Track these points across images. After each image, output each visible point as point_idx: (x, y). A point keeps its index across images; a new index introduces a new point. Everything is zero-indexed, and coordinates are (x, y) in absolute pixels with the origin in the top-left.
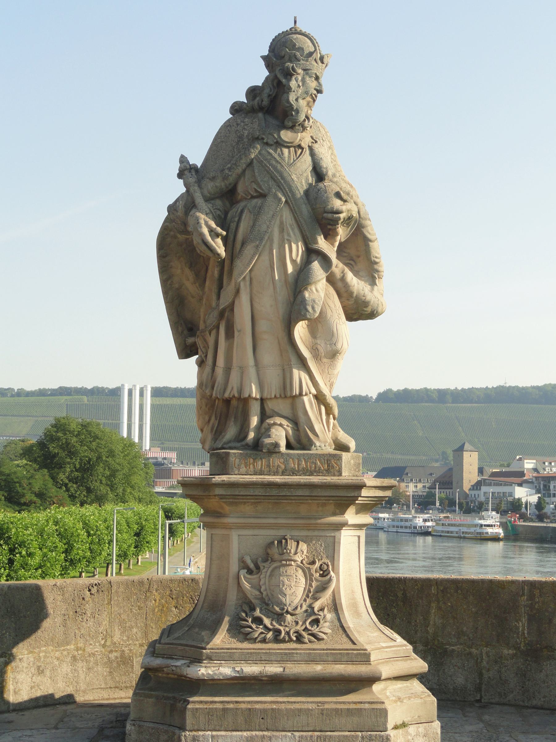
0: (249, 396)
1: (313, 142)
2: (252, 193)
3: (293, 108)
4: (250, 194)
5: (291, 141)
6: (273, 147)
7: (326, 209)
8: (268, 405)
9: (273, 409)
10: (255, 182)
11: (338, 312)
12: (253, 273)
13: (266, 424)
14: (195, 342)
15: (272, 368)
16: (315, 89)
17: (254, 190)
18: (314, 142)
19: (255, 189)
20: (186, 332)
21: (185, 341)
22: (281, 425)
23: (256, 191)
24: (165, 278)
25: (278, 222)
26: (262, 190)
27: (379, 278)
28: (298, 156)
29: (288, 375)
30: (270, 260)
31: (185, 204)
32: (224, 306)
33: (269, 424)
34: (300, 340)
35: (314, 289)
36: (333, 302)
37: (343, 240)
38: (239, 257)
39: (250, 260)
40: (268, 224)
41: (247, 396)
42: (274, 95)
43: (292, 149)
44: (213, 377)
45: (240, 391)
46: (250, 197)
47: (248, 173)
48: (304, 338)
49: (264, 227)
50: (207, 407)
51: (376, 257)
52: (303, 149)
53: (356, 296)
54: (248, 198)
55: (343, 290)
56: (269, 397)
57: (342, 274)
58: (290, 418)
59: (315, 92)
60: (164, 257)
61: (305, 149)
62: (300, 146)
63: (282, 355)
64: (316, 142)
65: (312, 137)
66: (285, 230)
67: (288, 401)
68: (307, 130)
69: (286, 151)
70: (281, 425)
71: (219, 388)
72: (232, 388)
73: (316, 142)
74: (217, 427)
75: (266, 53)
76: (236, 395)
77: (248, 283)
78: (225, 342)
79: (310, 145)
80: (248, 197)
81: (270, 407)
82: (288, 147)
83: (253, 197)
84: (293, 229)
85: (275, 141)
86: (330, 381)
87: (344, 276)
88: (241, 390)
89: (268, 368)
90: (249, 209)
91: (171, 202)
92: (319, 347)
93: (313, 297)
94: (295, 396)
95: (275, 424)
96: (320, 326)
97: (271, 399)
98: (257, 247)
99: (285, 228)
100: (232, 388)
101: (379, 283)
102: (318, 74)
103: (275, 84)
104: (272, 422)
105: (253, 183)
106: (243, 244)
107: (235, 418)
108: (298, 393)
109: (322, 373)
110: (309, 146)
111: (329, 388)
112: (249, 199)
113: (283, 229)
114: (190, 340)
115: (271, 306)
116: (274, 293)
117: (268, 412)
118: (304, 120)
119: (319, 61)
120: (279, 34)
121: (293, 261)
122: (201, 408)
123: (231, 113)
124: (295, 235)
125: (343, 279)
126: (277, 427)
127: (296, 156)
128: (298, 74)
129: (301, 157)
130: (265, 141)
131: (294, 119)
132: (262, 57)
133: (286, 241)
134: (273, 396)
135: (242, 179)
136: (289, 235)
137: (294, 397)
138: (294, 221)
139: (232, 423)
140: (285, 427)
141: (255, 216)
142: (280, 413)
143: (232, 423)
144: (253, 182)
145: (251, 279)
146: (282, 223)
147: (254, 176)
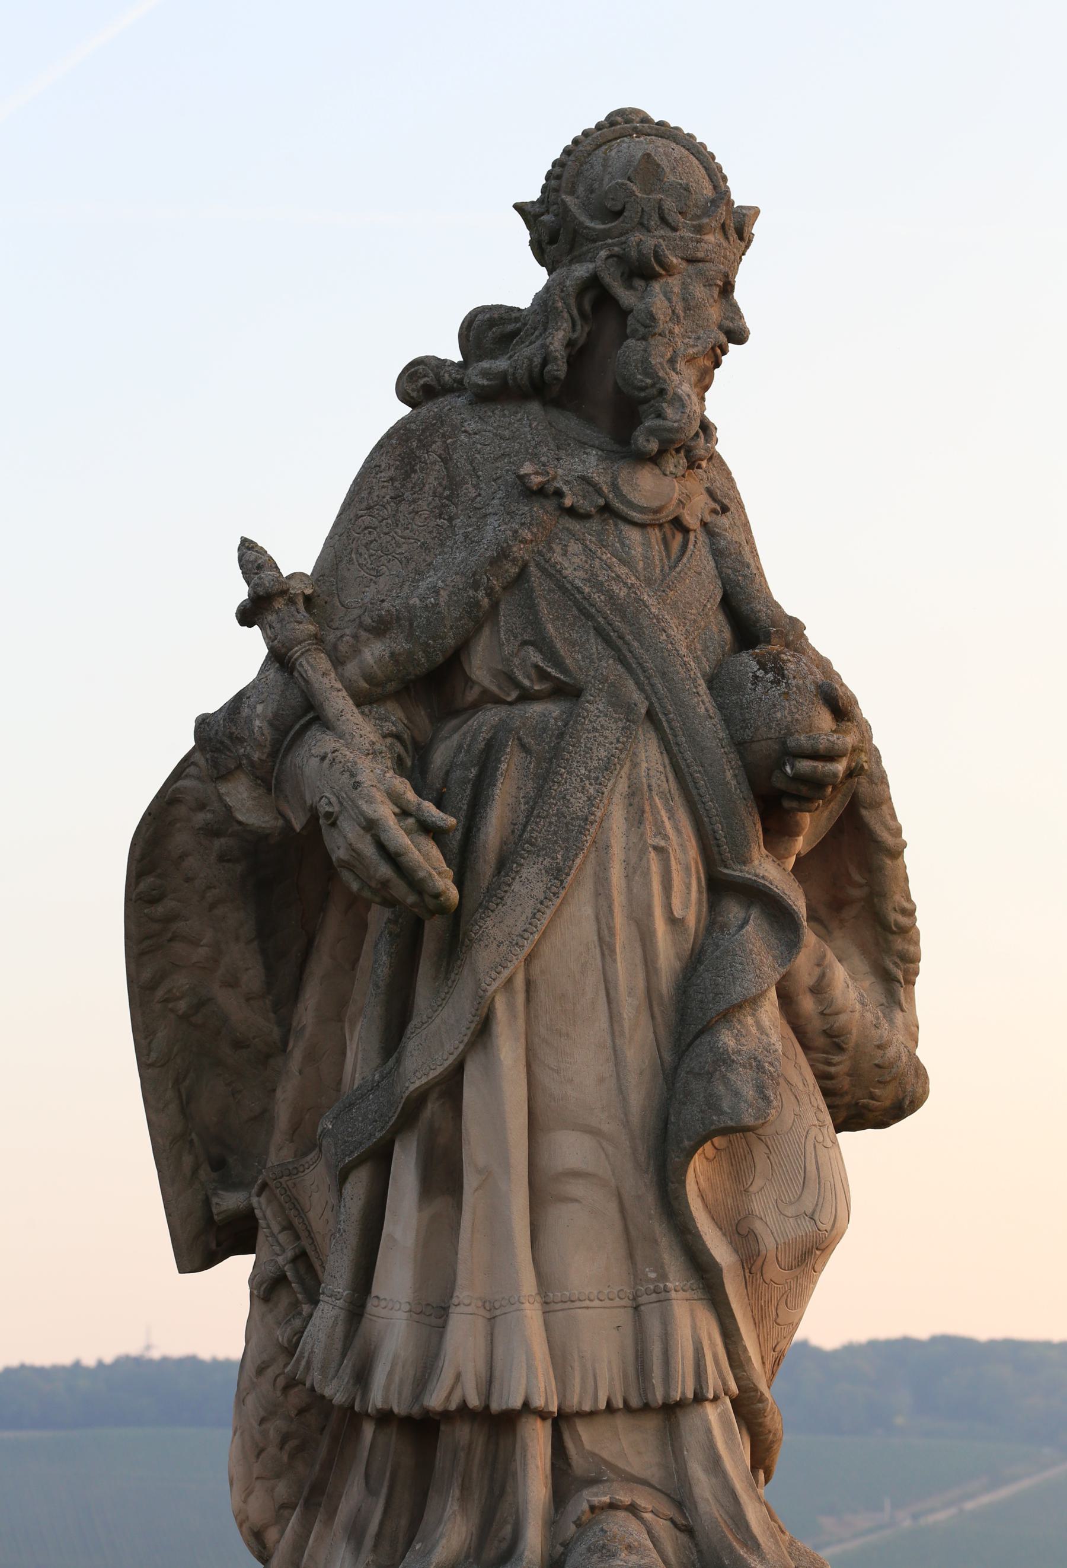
0: (526, 1404)
1: (714, 511)
2: (526, 683)
3: (662, 392)
4: (517, 685)
5: (656, 504)
6: (594, 525)
7: (791, 742)
8: (577, 1440)
9: (596, 1451)
10: (542, 643)
11: (815, 1105)
12: (537, 966)
13: (585, 1506)
14: (251, 1210)
15: (596, 1303)
16: (720, 327)
17: (533, 672)
19: (536, 667)
20: (205, 1172)
21: (207, 1203)
22: (633, 1509)
23: (543, 675)
24: (146, 975)
25: (622, 786)
26: (565, 670)
28: (674, 557)
29: (654, 1328)
30: (598, 920)
31: (276, 715)
32: (424, 1080)
33: (593, 1508)
34: (699, 1201)
35: (750, 1020)
36: (797, 1066)
38: (492, 906)
39: (534, 916)
40: (591, 791)
41: (517, 1403)
42: (581, 342)
43: (655, 535)
44: (358, 1343)
45: (489, 1383)
46: (514, 695)
47: (508, 616)
48: (709, 1196)
49: (578, 802)
50: (287, 1447)
52: (686, 531)
53: (857, 1045)
54: (509, 699)
55: (815, 1025)
56: (587, 1407)
57: (817, 971)
58: (654, 1481)
59: (723, 338)
60: (153, 901)
61: (692, 536)
62: (677, 523)
63: (631, 1256)
64: (725, 509)
65: (710, 493)
66: (648, 815)
67: (651, 1424)
68: (699, 467)
69: (634, 535)
70: (633, 1509)
71: (397, 1379)
72: (458, 1377)
73: (725, 509)
74: (382, 1524)
75: (533, 194)
76: (474, 1401)
77: (520, 998)
78: (420, 1209)
79: (708, 518)
80: (509, 695)
81: (588, 1446)
82: (642, 526)
83: (527, 697)
84: (671, 812)
85: (601, 502)
86: (778, 1349)
87: (823, 975)
88: (490, 1382)
89: (587, 1303)
90: (519, 739)
91: (214, 702)
92: (758, 1227)
93: (750, 1045)
94: (681, 1404)
95: (613, 1506)
96: (760, 1151)
97: (592, 1414)
98: (558, 874)
99: (647, 808)
100: (458, 1377)
103: (587, 306)
104: (606, 1499)
105: (531, 649)
106: (504, 864)
107: (463, 1488)
108: (690, 1395)
109: (758, 1321)
110: (704, 524)
111: (769, 1372)
112: (510, 704)
113: (643, 812)
114: (230, 1201)
115: (601, 1080)
116: (613, 1034)
117: (578, 1463)
118: (697, 435)
119: (732, 232)
120: (586, 133)
121: (674, 922)
122: (260, 1452)
123: (404, 396)
124: (678, 831)
126: (622, 1514)
127: (668, 556)
128: (669, 270)
129: (685, 560)
130: (568, 502)
131: (670, 430)
132: (519, 208)
133: (653, 854)
134: (602, 1405)
135: (486, 631)
136: (660, 832)
137: (671, 1410)
138: (673, 785)
139: (452, 1506)
140: (648, 1516)
141: (544, 765)
142: (621, 1464)
143: (452, 1506)
144: (525, 643)
145: (529, 984)
146: (633, 792)
147: (536, 624)
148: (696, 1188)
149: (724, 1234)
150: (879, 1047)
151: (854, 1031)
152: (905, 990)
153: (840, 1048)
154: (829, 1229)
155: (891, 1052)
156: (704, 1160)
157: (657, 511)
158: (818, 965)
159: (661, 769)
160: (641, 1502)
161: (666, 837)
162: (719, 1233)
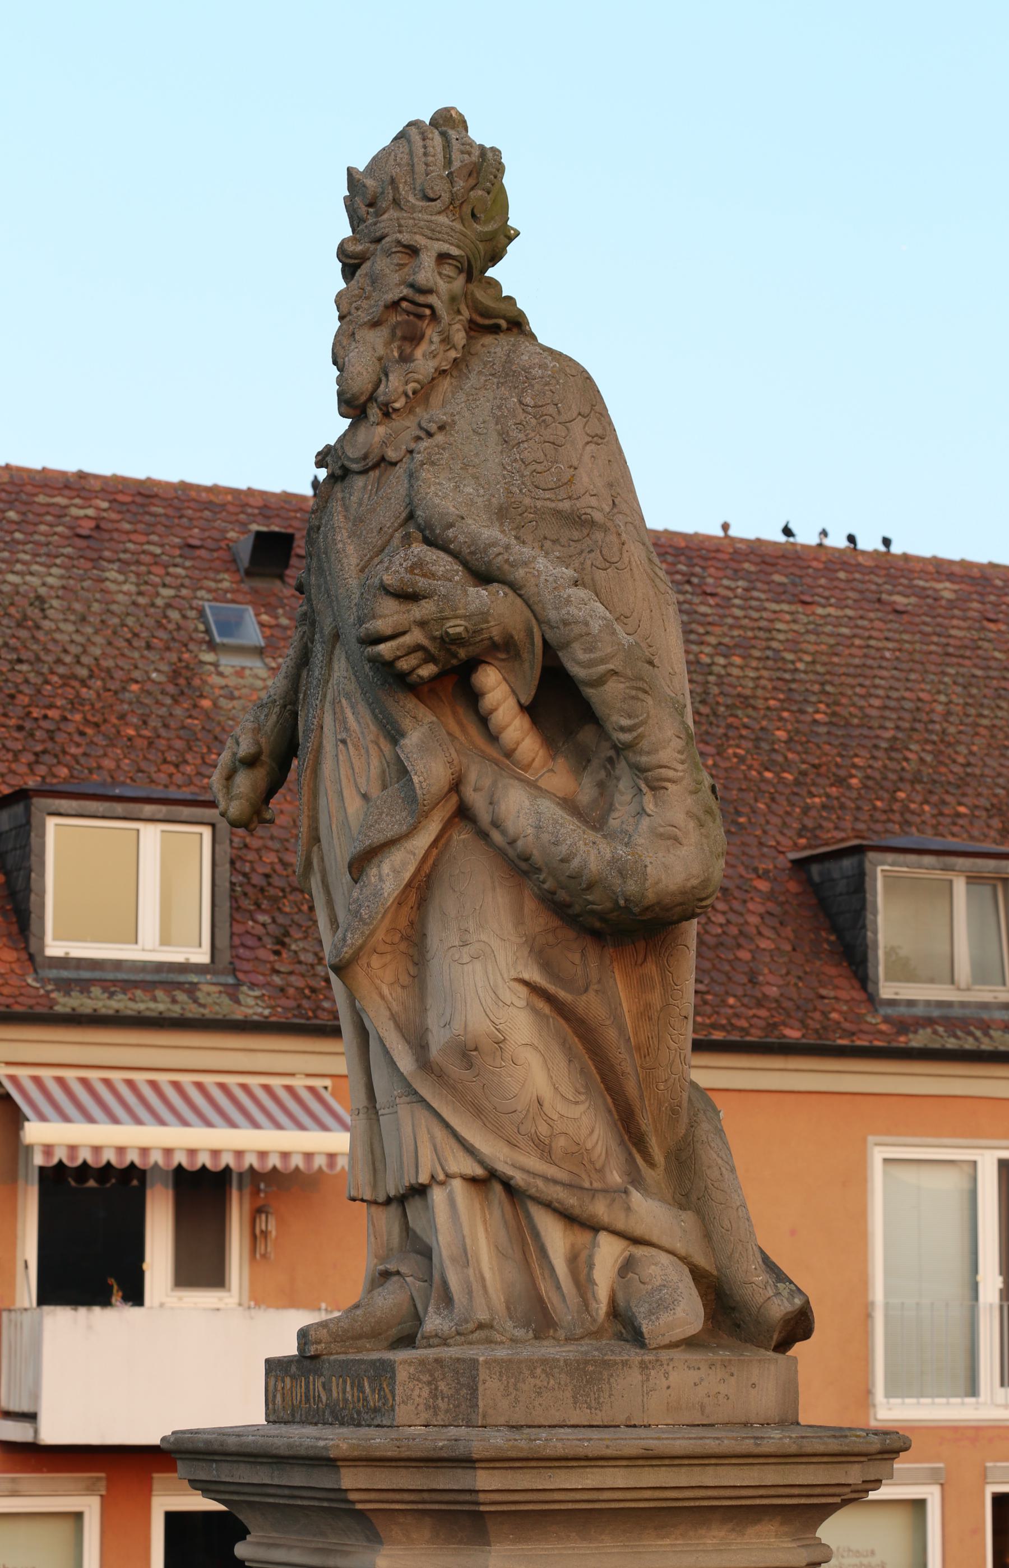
18: (422, 434)
27: (652, 788)
37: (526, 699)
51: (623, 729)
73: (430, 435)
101: (656, 805)
102: (405, 238)
109: (477, 1111)
125: (496, 824)
148: (388, 1013)
149: (411, 1048)
150: (562, 861)
151: (535, 852)
152: (654, 796)
153: (539, 870)
154: (462, 1033)
155: (575, 863)
156: (399, 990)
157: (365, 457)
158: (491, 803)
159: (345, 674)
160: (403, 1270)
161: (347, 729)
162: (407, 1047)
